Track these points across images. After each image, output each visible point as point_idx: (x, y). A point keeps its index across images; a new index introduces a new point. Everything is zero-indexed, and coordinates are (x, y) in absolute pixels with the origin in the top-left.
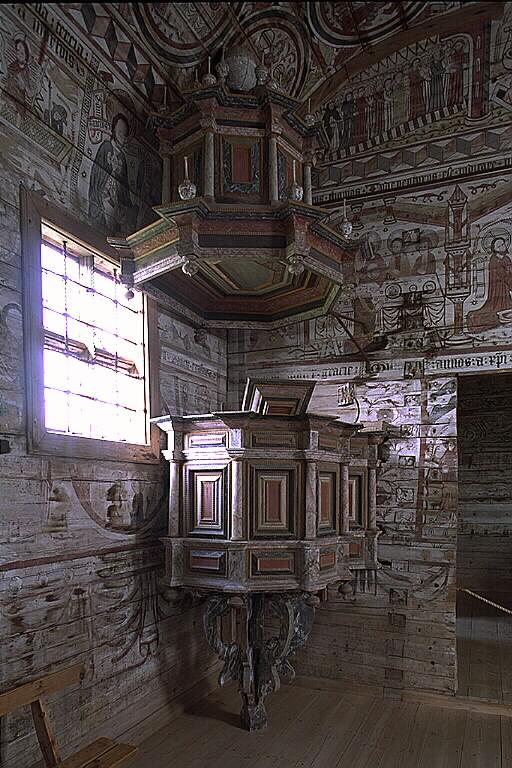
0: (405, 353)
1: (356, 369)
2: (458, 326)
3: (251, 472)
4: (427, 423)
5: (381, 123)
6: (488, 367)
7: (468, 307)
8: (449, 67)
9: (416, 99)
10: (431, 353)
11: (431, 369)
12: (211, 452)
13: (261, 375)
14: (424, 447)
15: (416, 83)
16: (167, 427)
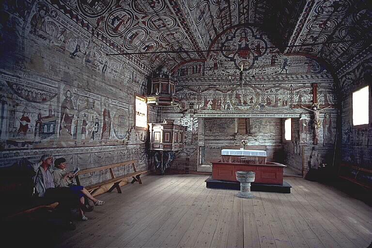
0: (191, 112)
1: (182, 115)
2: (199, 109)
3: (164, 132)
4: (193, 125)
5: (187, 73)
6: (203, 116)
7: (200, 106)
8: (199, 67)
9: (193, 71)
10: (194, 113)
11: (194, 116)
12: (158, 131)
13: (166, 118)
14: (193, 129)
15: (193, 68)
16: (150, 125)
